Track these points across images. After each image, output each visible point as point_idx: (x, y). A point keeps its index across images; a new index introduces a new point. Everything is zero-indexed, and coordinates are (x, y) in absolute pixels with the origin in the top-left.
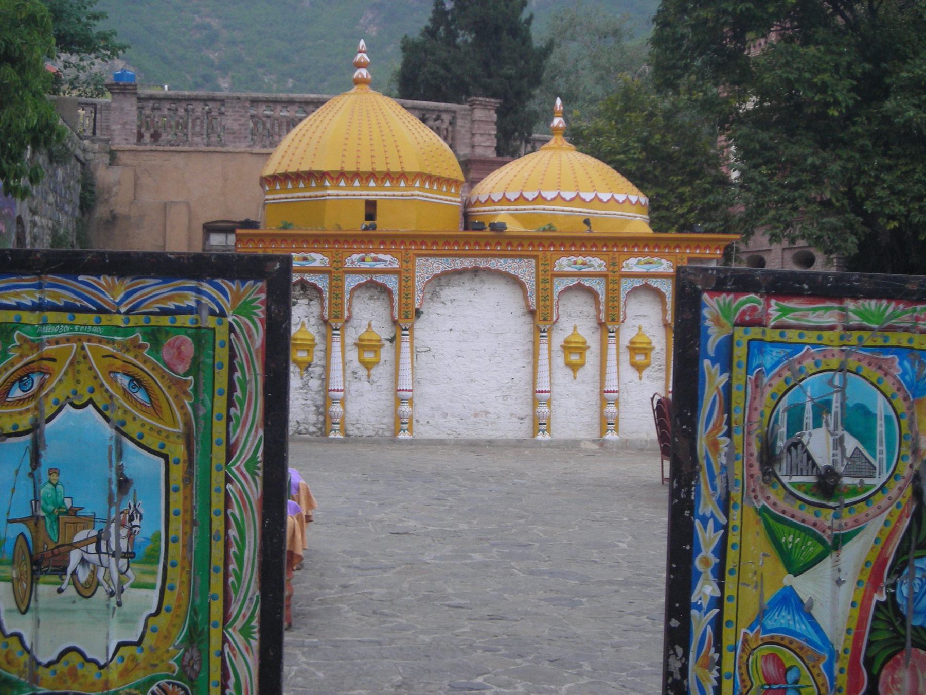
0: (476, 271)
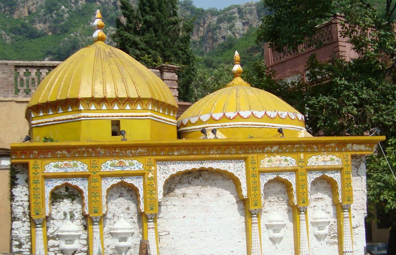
0: (201, 171)
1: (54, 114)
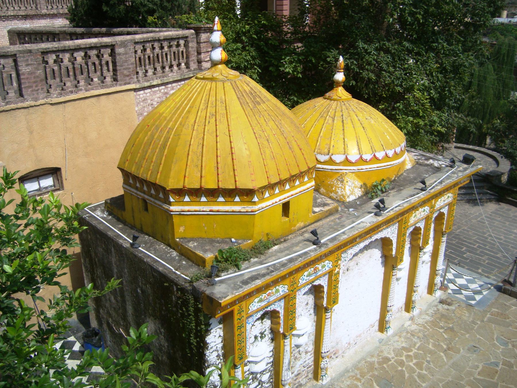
1: (208, 201)
